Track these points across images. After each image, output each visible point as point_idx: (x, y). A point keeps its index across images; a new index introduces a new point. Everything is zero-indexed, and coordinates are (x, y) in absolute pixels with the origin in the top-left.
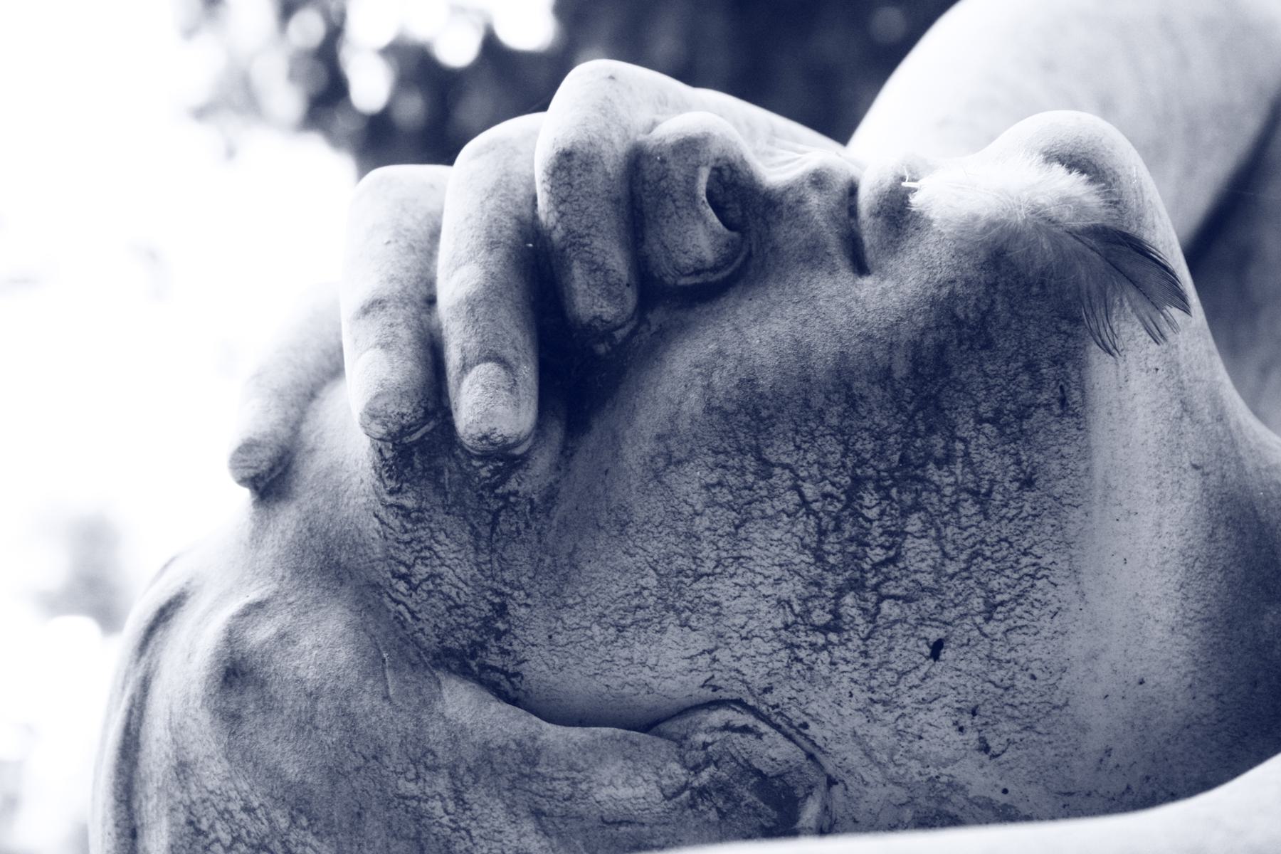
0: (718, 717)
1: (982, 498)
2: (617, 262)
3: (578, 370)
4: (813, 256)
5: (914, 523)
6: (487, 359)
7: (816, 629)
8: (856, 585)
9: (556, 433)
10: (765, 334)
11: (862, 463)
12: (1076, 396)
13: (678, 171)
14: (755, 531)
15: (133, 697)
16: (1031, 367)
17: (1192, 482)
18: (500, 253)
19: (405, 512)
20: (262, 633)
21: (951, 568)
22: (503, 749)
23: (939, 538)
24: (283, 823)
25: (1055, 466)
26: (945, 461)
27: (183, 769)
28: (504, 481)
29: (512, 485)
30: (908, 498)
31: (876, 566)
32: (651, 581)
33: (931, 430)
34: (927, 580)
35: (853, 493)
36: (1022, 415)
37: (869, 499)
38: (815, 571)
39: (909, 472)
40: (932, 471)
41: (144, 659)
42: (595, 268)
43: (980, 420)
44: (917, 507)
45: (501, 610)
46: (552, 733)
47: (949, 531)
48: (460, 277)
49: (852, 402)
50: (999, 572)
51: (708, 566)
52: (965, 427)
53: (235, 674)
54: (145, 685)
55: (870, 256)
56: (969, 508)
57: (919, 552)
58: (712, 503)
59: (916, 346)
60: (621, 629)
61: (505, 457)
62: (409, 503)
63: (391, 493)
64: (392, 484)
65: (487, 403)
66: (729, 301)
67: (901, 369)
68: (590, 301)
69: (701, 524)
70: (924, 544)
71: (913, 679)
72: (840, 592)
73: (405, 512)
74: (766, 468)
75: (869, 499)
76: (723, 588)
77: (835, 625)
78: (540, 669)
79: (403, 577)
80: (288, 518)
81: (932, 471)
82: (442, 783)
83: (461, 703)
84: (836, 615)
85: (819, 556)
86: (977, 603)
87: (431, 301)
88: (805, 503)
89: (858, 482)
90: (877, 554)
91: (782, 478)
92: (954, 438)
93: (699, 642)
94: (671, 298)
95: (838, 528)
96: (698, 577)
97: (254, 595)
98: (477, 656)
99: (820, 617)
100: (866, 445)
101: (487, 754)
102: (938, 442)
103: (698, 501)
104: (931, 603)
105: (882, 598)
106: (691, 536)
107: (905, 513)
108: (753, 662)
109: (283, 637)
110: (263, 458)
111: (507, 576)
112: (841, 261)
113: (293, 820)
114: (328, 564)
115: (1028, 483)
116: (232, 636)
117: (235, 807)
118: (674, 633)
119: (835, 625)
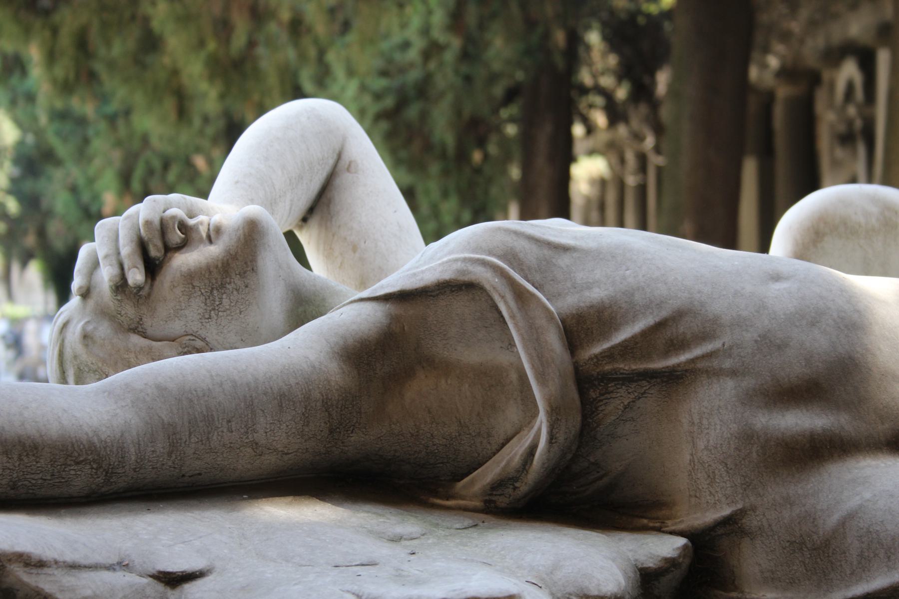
0: (188, 338)
1: (237, 290)
2: (160, 244)
3: (152, 268)
4: (201, 241)
5: (224, 296)
8: (214, 309)
9: (149, 281)
13: (171, 223)
14: (192, 300)
16: (246, 263)
19: (119, 300)
20: (90, 328)
24: (100, 365)
26: (230, 283)
27: (75, 357)
35: (211, 292)
36: (245, 273)
37: (215, 292)
39: (223, 286)
40: (228, 286)
42: (155, 246)
45: (141, 319)
46: (154, 343)
48: (127, 249)
49: (210, 272)
52: (233, 277)
53: (86, 337)
54: (63, 341)
56: (235, 292)
57: (226, 302)
59: (223, 260)
61: (140, 288)
62: (119, 298)
65: (136, 276)
66: (184, 250)
67: (220, 265)
68: (154, 252)
73: (119, 300)
74: (194, 287)
75: (215, 292)
76: (187, 312)
77: (210, 318)
78: (150, 331)
80: (91, 303)
81: (228, 286)
82: (132, 355)
83: (136, 339)
85: (206, 305)
87: (119, 253)
89: (213, 289)
90: (217, 303)
91: (197, 289)
93: (183, 323)
97: (86, 320)
98: (137, 329)
99: (207, 316)
100: (214, 281)
101: (141, 349)
102: (228, 280)
103: (180, 294)
106: (180, 302)
108: (194, 327)
109: (95, 328)
110: (84, 290)
112: (207, 242)
114: (102, 313)
115: (247, 286)
116: (84, 329)
117: (89, 363)
118: (177, 321)
119: (210, 318)
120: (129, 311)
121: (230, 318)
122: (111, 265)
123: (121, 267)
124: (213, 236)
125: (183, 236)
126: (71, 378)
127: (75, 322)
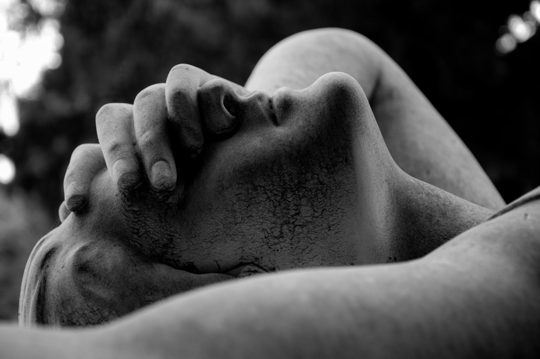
2: (196, 127)
5: (304, 201)
6: (160, 160)
7: (276, 237)
10: (252, 144)
11: (285, 183)
12: (350, 158)
15: (41, 283)
17: (385, 186)
18: (158, 127)
19: (135, 212)
21: (316, 215)
22: (179, 283)
23: (312, 205)
25: (345, 181)
28: (167, 199)
29: (170, 200)
30: (301, 194)
31: (292, 216)
32: (221, 227)
33: (307, 172)
34: (309, 219)
35: (283, 194)
36: (334, 165)
38: (274, 219)
41: (43, 271)
43: (321, 168)
44: (304, 196)
47: (315, 204)
50: (332, 215)
51: (239, 220)
55: (279, 120)
56: (320, 196)
58: (239, 200)
60: (212, 243)
62: (136, 209)
63: (129, 206)
64: (129, 203)
69: (236, 207)
70: (308, 208)
71: (307, 251)
72: (282, 225)
73: (135, 212)
79: (137, 233)
84: (282, 233)
86: (325, 226)
87: (134, 144)
88: (269, 198)
90: (293, 212)
92: (314, 174)
94: (214, 138)
95: (280, 205)
96: (236, 224)
100: (287, 178)
104: (311, 227)
105: (295, 226)
107: (300, 199)
111: (172, 229)
112: (270, 122)
113: (110, 312)
120: (153, 228)
121: (313, 236)
122: (123, 158)
123: (138, 158)
124: (278, 116)
125: (234, 117)
126: (52, 315)
127: (65, 248)
